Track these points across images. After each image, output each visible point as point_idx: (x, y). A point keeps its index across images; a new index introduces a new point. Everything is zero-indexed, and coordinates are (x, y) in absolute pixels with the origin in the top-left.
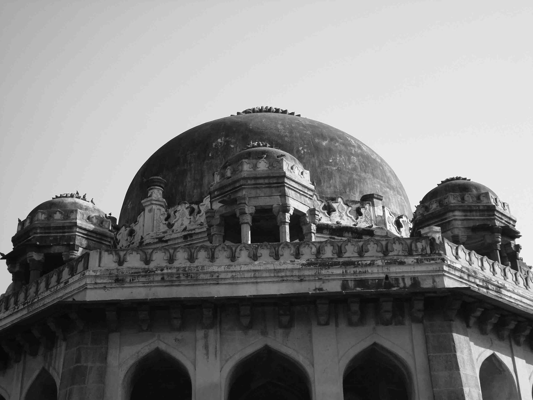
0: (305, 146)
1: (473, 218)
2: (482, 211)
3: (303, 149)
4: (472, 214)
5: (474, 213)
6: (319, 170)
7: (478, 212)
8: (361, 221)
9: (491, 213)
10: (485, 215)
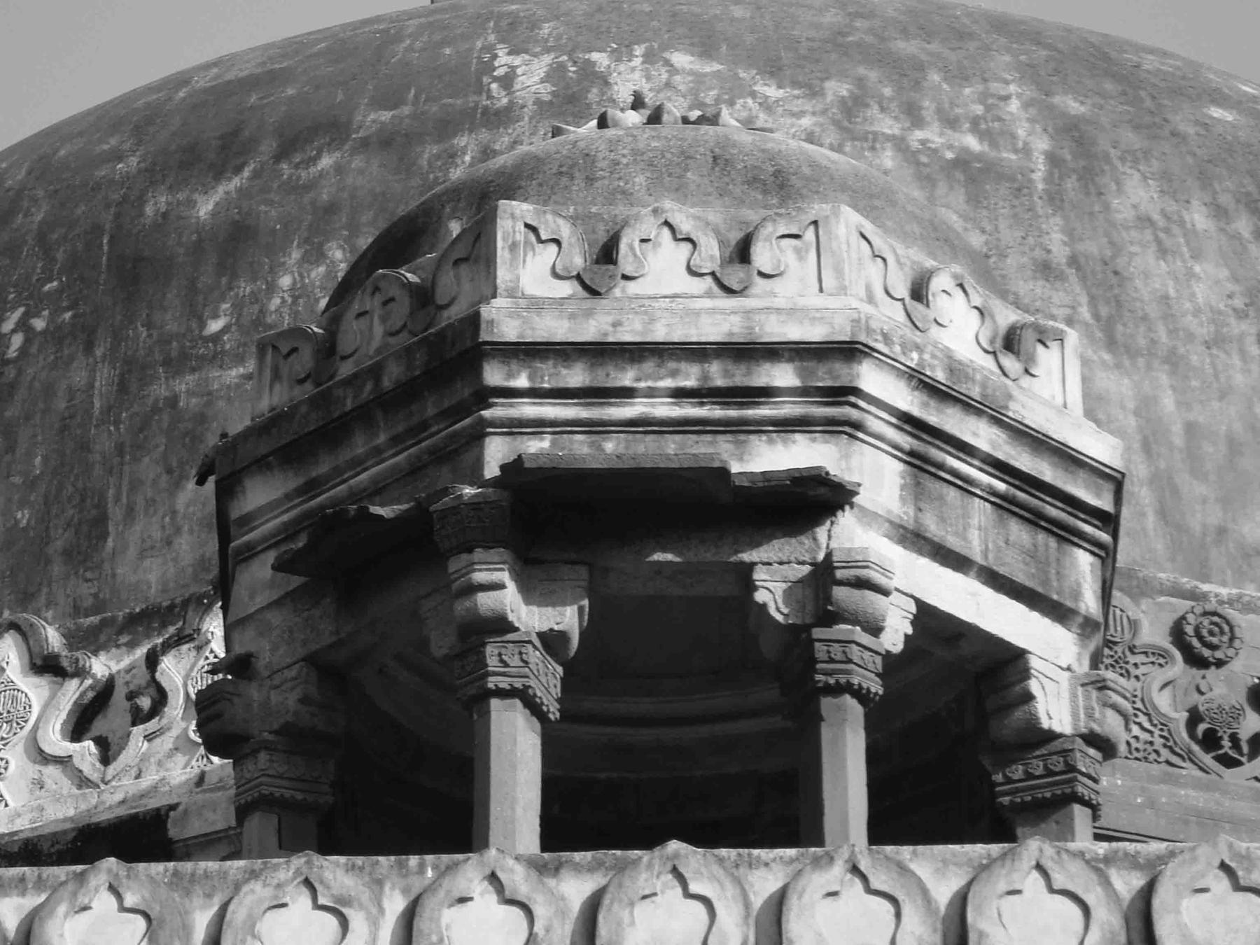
0: (47, 287)
1: (364, 476)
2: (408, 393)
3: (23, 325)
4: (345, 455)
5: (359, 445)
6: (104, 443)
7: (379, 415)
8: (144, 758)
9: (464, 391)
10: (424, 426)
